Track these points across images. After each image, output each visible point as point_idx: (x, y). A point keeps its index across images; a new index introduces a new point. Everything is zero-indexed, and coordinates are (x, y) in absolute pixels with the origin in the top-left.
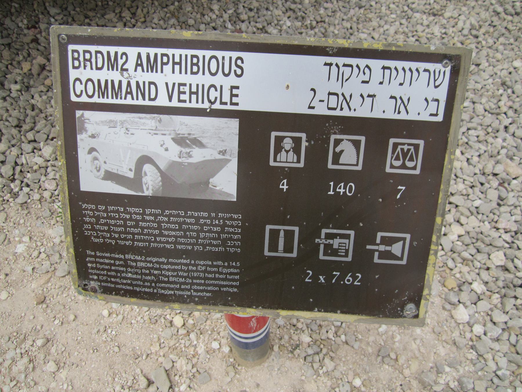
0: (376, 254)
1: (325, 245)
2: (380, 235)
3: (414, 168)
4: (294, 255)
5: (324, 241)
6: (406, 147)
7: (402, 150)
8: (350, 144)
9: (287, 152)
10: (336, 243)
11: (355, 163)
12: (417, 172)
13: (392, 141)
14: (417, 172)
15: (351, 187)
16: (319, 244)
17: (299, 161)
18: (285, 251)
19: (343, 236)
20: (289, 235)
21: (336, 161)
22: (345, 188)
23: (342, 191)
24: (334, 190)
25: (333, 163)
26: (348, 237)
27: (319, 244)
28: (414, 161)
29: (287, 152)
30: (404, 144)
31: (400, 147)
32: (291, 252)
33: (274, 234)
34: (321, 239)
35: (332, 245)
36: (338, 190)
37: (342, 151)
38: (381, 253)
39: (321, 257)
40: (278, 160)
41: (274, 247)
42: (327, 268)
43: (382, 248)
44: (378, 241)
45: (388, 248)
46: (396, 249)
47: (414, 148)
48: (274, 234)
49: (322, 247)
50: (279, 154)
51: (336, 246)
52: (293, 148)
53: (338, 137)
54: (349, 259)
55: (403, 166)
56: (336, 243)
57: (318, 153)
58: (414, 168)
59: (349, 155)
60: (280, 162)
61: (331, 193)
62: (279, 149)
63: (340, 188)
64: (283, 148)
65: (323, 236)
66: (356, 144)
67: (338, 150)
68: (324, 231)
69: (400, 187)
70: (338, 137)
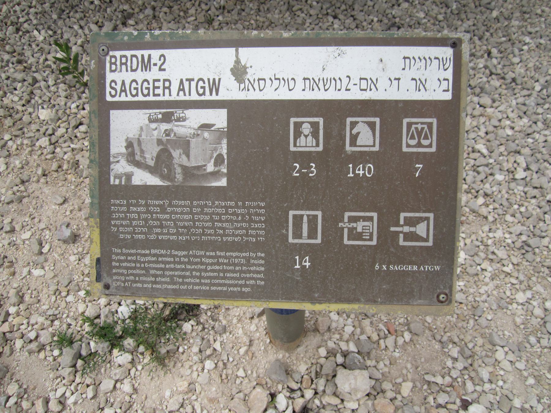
0: (401, 236)
1: (349, 228)
2: (403, 215)
3: (430, 146)
4: (319, 241)
5: (347, 224)
6: (419, 126)
7: (416, 128)
8: (366, 125)
9: (306, 136)
10: (359, 226)
11: (372, 144)
12: (433, 149)
13: (405, 121)
14: (433, 149)
15: (369, 168)
16: (343, 229)
17: (317, 145)
18: (309, 237)
19: (365, 219)
20: (313, 220)
21: (353, 143)
22: (364, 169)
23: (361, 172)
24: (354, 172)
25: (351, 145)
26: (371, 219)
27: (343, 229)
28: (428, 139)
29: (306, 136)
30: (417, 123)
31: (414, 126)
32: (316, 238)
34: (345, 223)
35: (356, 228)
36: (357, 172)
37: (358, 133)
38: (405, 234)
39: (346, 242)
40: (298, 144)
41: (298, 234)
43: (406, 229)
44: (402, 222)
45: (412, 229)
46: (421, 229)
47: (428, 127)
48: (298, 220)
49: (346, 231)
50: (298, 140)
51: (359, 230)
52: (311, 133)
53: (354, 119)
54: (374, 242)
55: (419, 145)
56: (359, 226)
57: (334, 137)
58: (430, 146)
60: (300, 147)
61: (351, 175)
62: (298, 134)
63: (359, 170)
64: (301, 133)
65: (346, 220)
66: (372, 126)
67: (354, 131)
68: (347, 215)
69: (417, 166)
70: (354, 119)
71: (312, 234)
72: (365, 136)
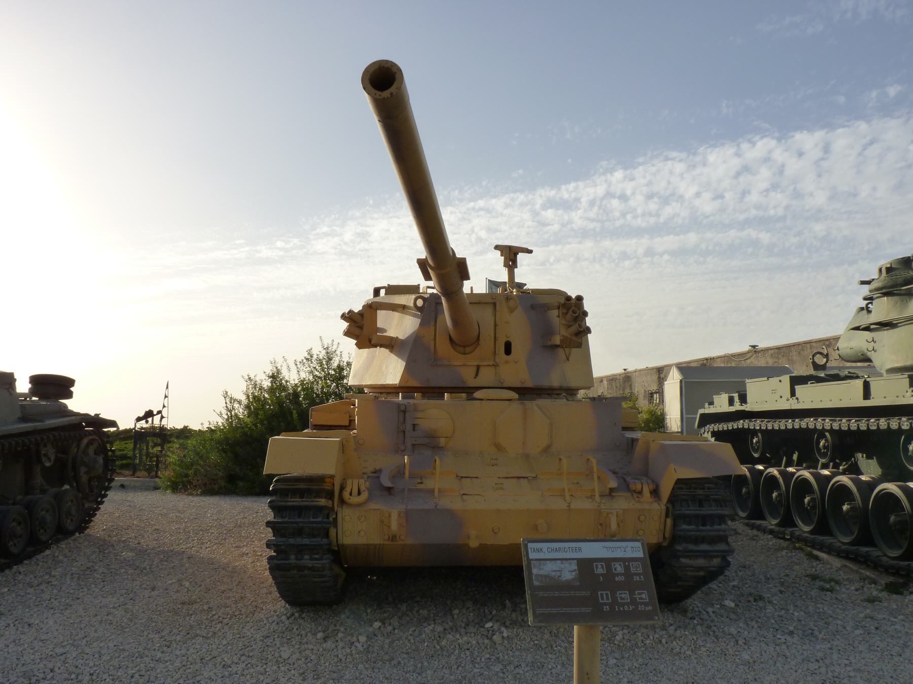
10: (623, 596)
33: (602, 595)
41: (602, 599)
42: (623, 605)
46: (643, 596)
48: (602, 595)
59: (619, 568)
71: (608, 598)
72: (619, 568)
